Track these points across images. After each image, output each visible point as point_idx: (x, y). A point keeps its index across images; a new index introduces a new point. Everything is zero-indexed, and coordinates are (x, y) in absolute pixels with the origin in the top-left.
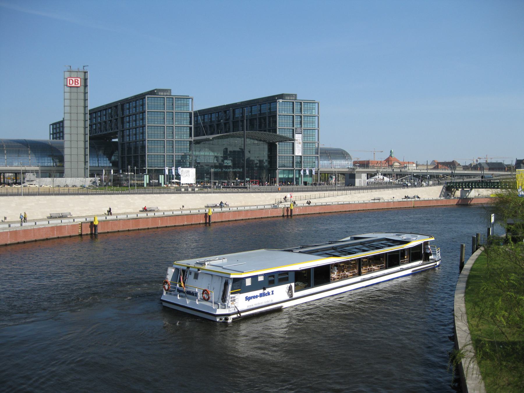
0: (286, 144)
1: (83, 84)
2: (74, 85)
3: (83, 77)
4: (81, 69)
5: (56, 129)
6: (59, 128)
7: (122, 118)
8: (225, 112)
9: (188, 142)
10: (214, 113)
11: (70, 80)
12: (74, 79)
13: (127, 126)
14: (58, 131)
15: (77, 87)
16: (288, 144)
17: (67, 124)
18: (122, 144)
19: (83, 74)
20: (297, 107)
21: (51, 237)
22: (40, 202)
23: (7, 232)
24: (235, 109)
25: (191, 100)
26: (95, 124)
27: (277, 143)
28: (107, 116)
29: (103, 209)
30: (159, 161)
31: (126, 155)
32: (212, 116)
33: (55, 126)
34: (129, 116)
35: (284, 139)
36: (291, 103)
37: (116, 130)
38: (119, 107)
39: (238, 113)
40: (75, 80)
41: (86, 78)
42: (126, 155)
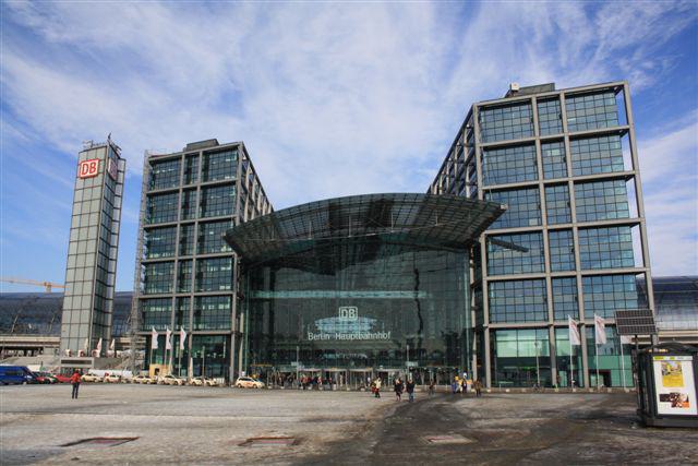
1: (101, 171)
2: (88, 174)
3: (102, 158)
12: (89, 163)
15: (94, 176)
27: (482, 240)
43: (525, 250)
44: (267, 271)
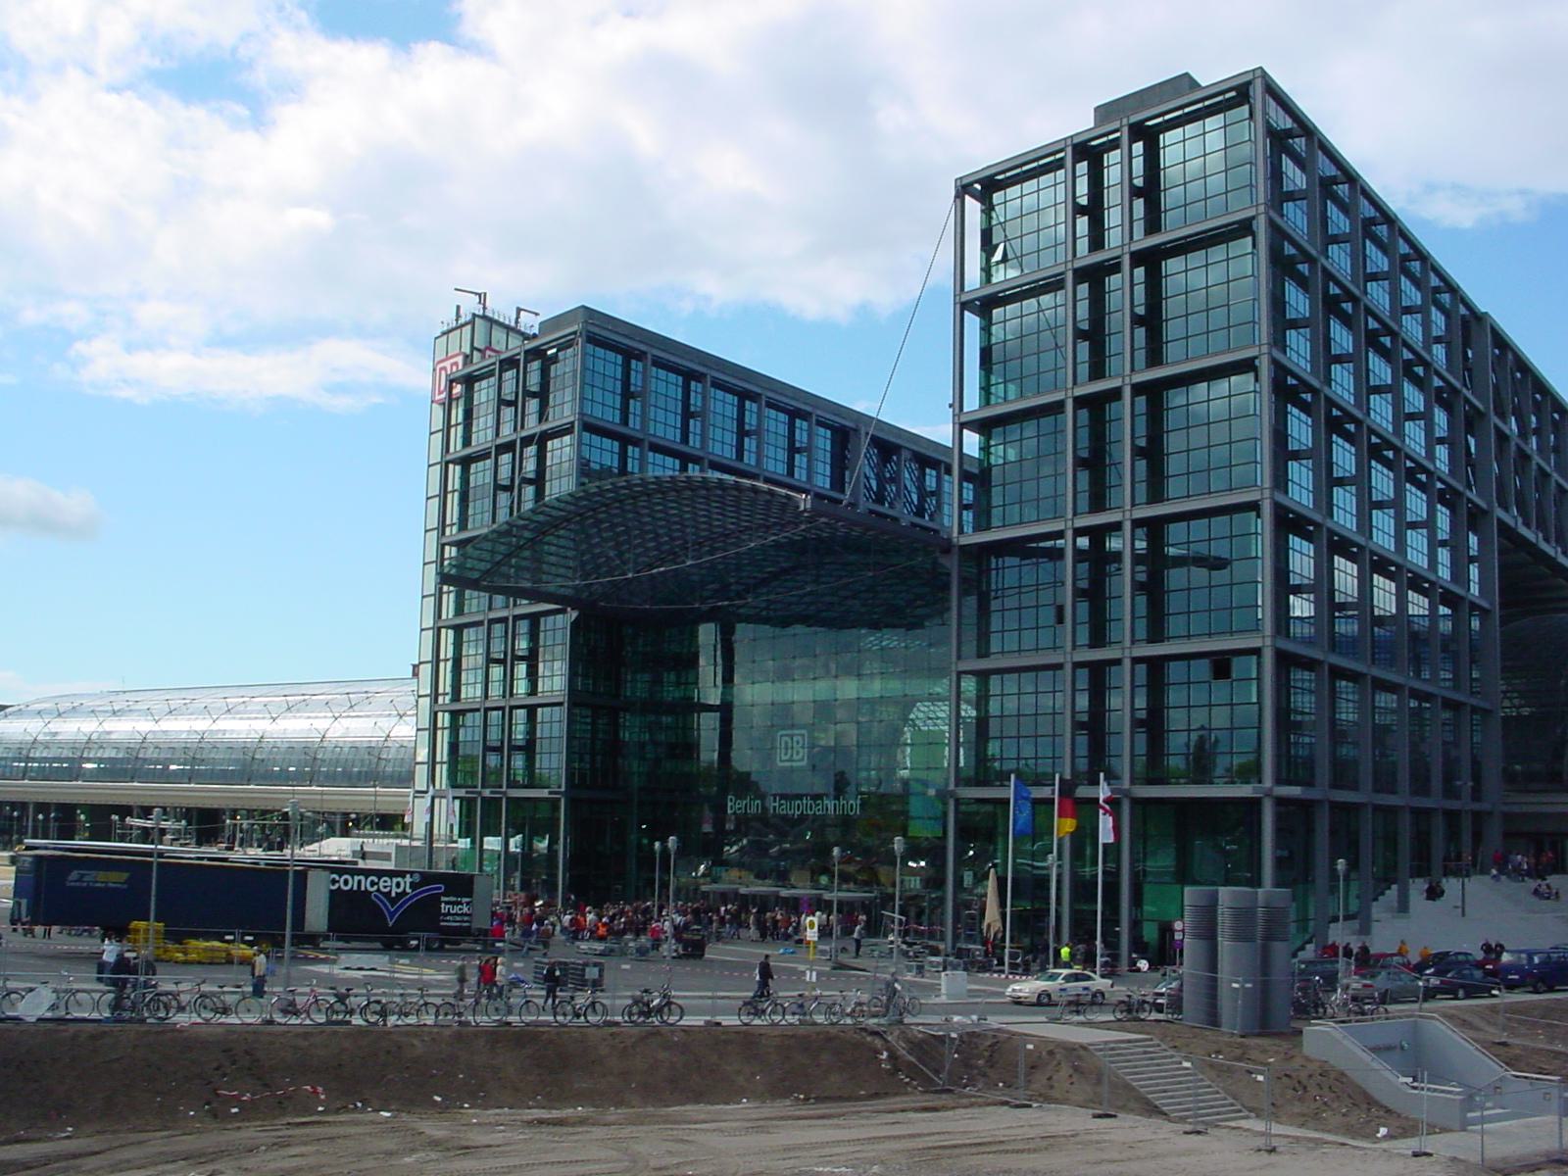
11: (441, 369)
40: (452, 365)
43: (1218, 564)
44: (707, 634)
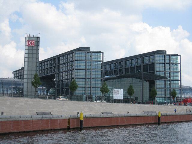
0: (160, 81)
1: (36, 44)
2: (31, 45)
4: (35, 36)
5: (17, 74)
6: (19, 73)
7: (58, 66)
8: (120, 63)
9: (100, 80)
10: (113, 64)
12: (31, 42)
13: (61, 70)
14: (18, 75)
15: (33, 46)
16: (162, 81)
17: (26, 68)
18: (58, 81)
19: (36, 38)
20: (167, 58)
21: (46, 129)
22: (28, 103)
23: (11, 121)
24: (126, 61)
25: (102, 54)
26: (41, 70)
28: (49, 65)
29: (74, 111)
30: (82, 91)
31: (61, 88)
32: (111, 66)
33: (16, 73)
34: (63, 64)
35: (160, 78)
36: (163, 56)
37: (54, 73)
38: (57, 59)
39: (128, 62)
40: (32, 42)
41: (38, 41)
42: (61, 88)
